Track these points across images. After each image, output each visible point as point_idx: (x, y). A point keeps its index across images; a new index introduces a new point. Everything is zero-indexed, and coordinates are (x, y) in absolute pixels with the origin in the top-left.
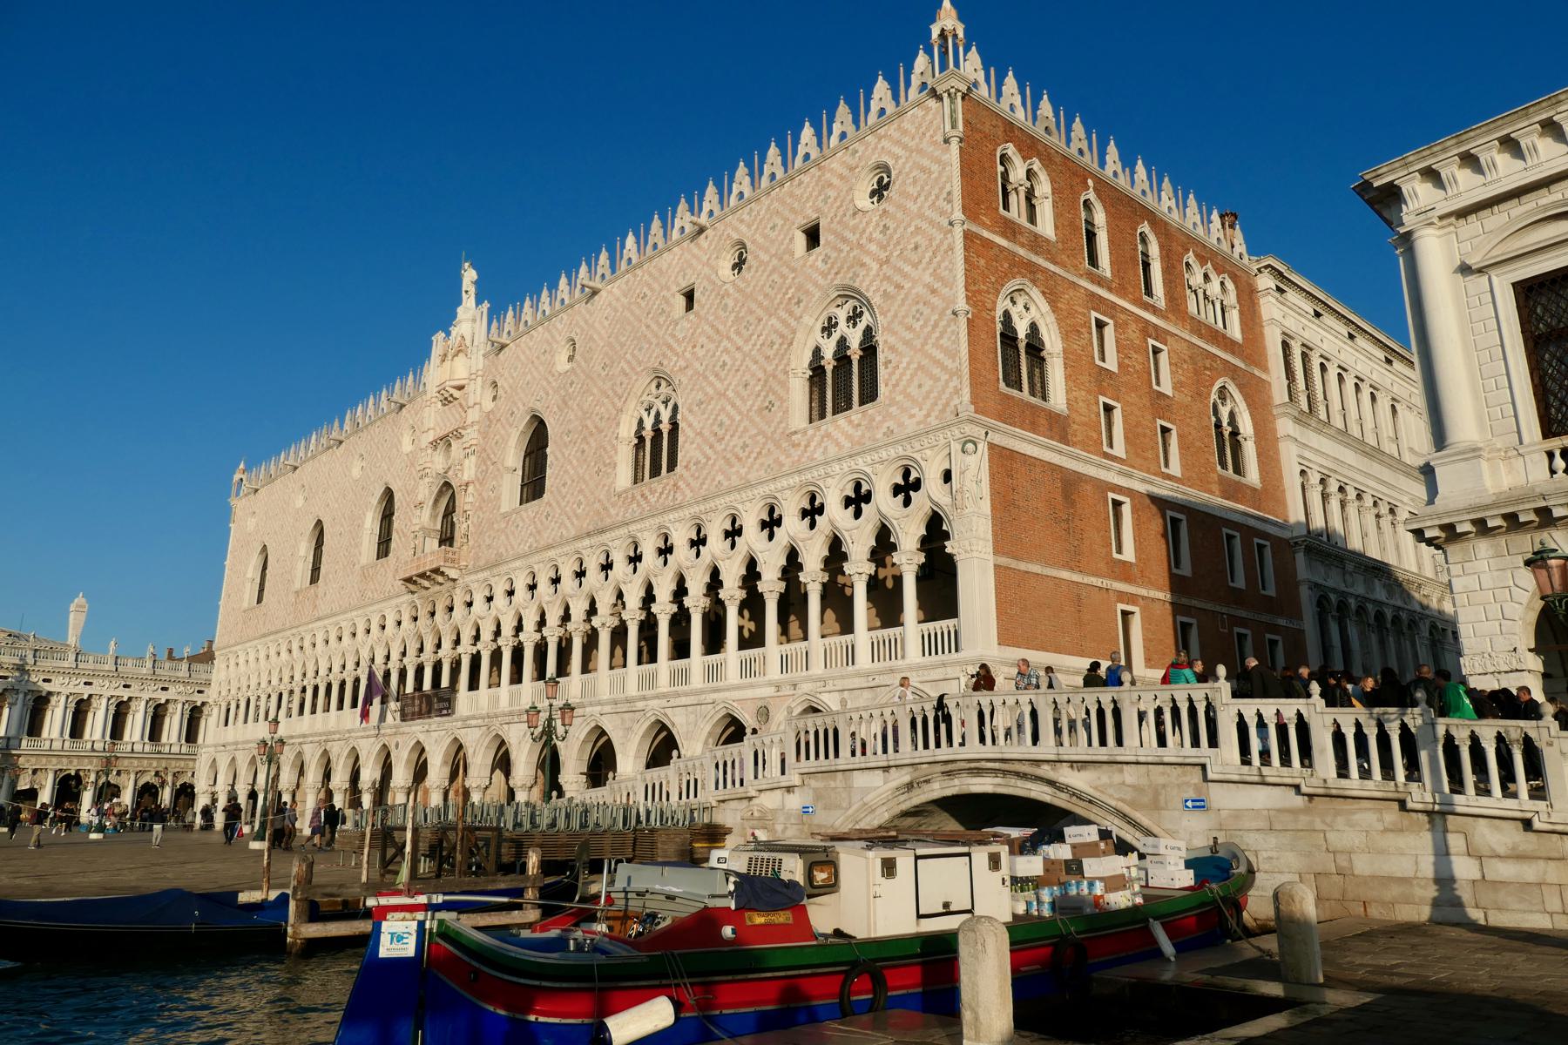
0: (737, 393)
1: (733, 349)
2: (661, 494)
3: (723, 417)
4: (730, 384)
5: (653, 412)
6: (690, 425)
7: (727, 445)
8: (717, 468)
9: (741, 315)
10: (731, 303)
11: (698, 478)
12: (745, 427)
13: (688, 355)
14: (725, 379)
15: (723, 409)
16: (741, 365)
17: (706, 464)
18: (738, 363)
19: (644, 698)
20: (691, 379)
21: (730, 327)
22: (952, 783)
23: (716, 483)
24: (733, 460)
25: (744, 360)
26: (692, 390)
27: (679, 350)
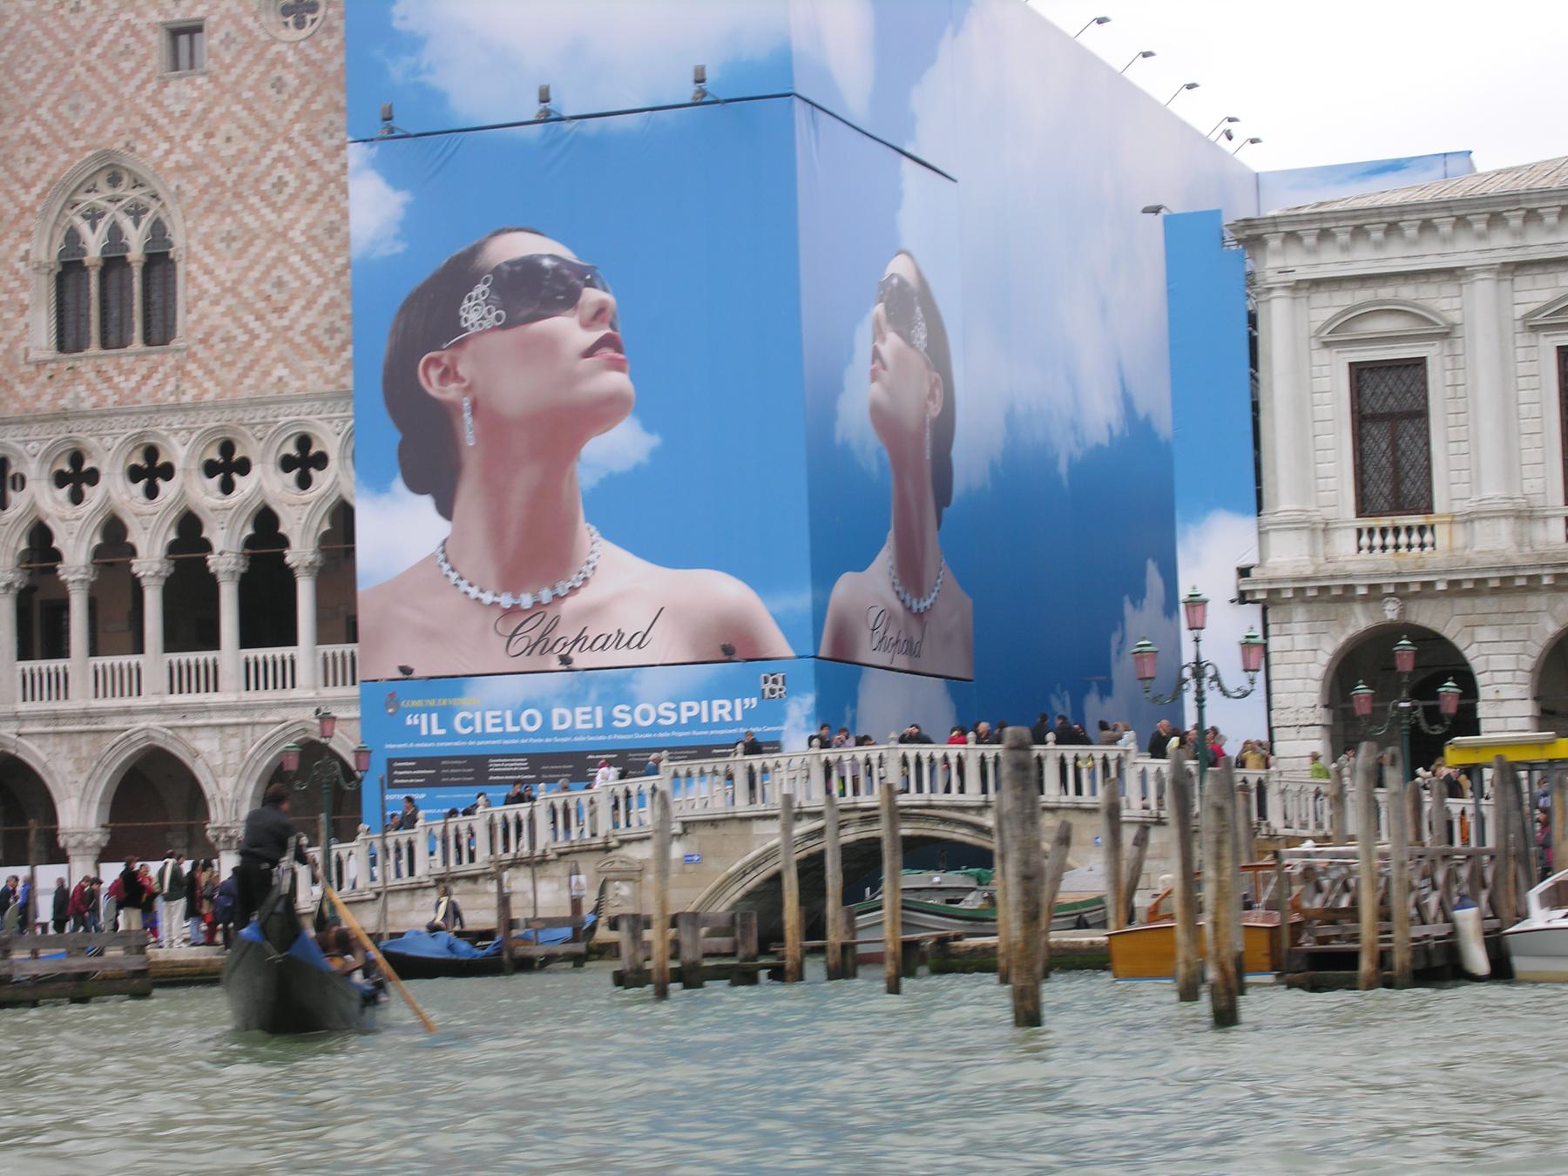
0: (313, 240)
1: (299, 163)
2: (146, 378)
3: (280, 271)
4: (297, 220)
5: (103, 226)
6: (208, 272)
7: (295, 320)
8: (273, 353)
9: (314, 107)
10: (291, 81)
11: (232, 364)
12: (332, 299)
13: (195, 145)
14: (284, 209)
15: (281, 259)
16: (318, 194)
17: (249, 344)
18: (313, 188)
19: (128, 712)
20: (204, 191)
21: (293, 122)
22: (867, 828)
23: (273, 379)
24: (309, 346)
25: (323, 187)
26: (209, 210)
27: (178, 134)
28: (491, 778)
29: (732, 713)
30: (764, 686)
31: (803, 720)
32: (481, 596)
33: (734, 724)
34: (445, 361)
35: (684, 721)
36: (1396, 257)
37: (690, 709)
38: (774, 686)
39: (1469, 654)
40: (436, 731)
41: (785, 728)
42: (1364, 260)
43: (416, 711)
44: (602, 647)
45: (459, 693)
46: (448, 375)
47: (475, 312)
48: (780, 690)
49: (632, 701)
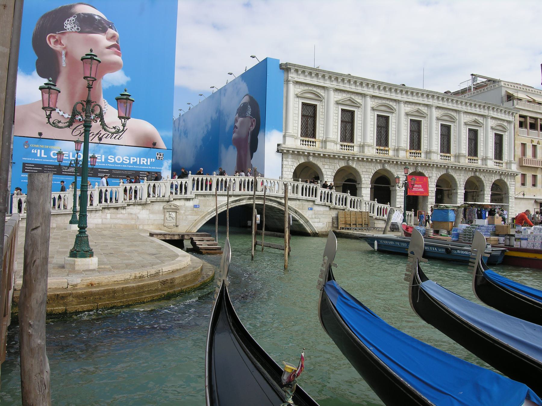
28: (63, 173)
29: (147, 162)
30: (157, 156)
31: (168, 167)
32: (64, 115)
33: (147, 165)
34: (57, 37)
35: (131, 163)
36: (315, 81)
37: (134, 159)
38: (160, 156)
39: (323, 170)
40: (43, 156)
41: (162, 168)
42: (308, 80)
43: (37, 149)
44: (106, 137)
45: (53, 145)
46: (57, 42)
47: (69, 25)
48: (162, 158)
49: (115, 155)
